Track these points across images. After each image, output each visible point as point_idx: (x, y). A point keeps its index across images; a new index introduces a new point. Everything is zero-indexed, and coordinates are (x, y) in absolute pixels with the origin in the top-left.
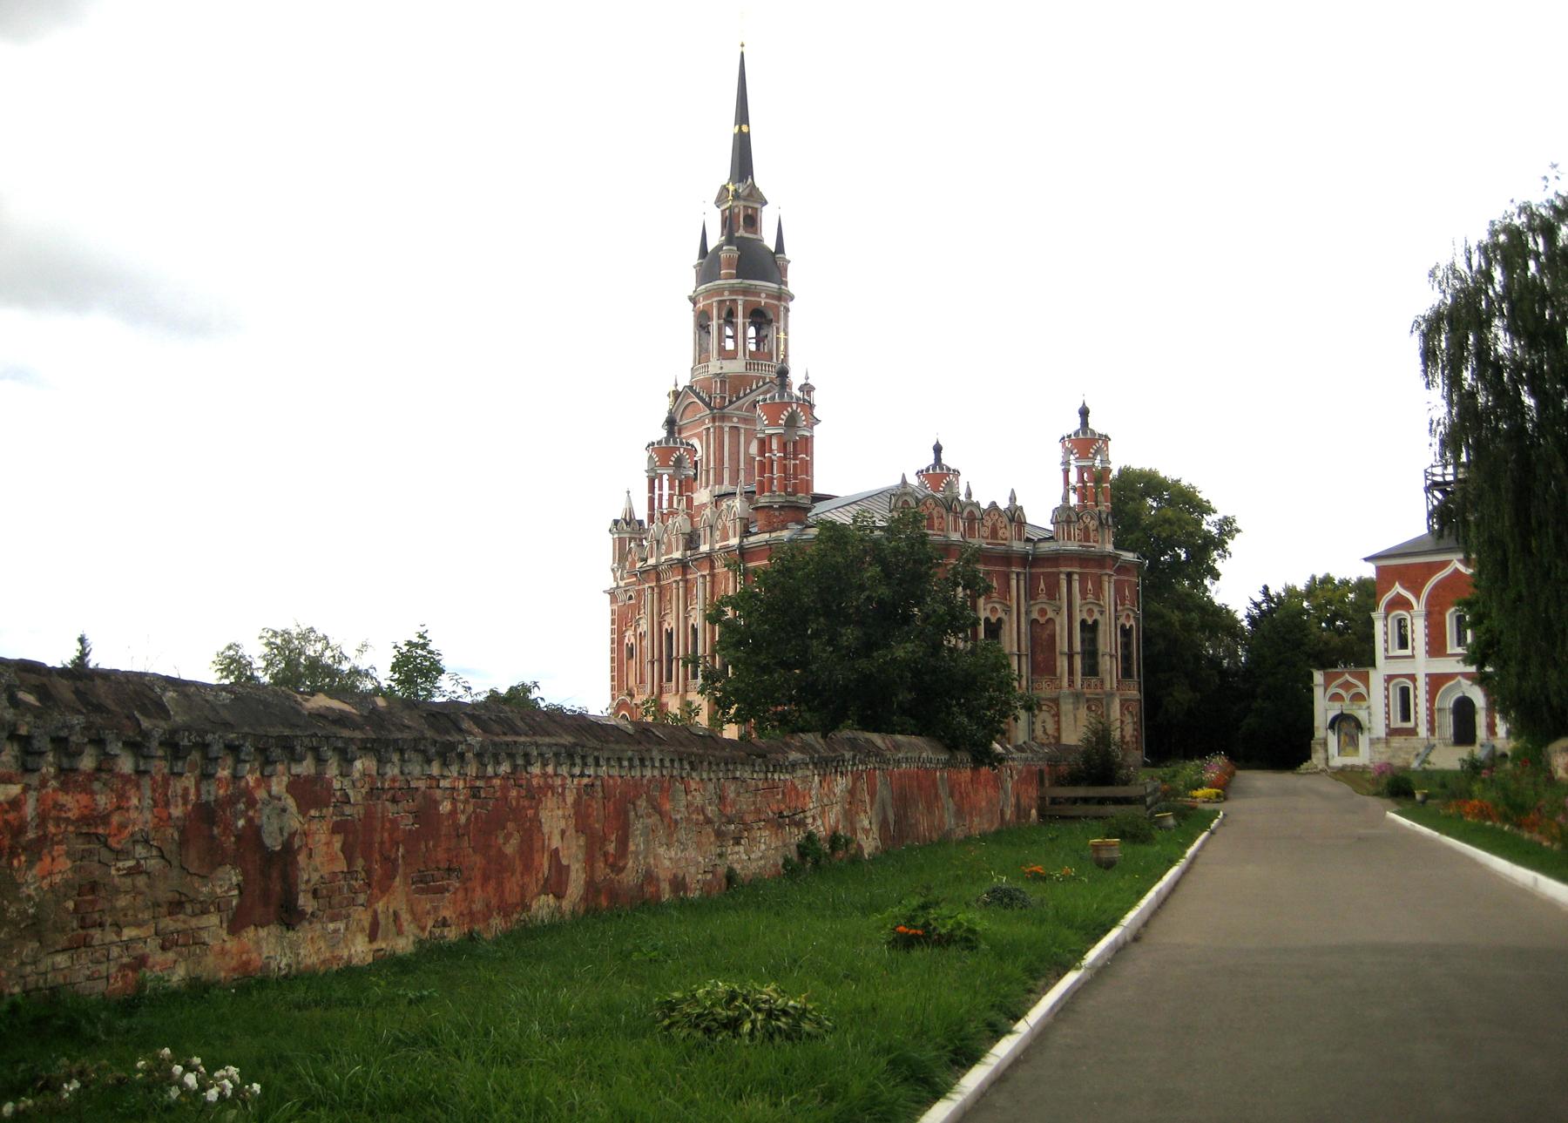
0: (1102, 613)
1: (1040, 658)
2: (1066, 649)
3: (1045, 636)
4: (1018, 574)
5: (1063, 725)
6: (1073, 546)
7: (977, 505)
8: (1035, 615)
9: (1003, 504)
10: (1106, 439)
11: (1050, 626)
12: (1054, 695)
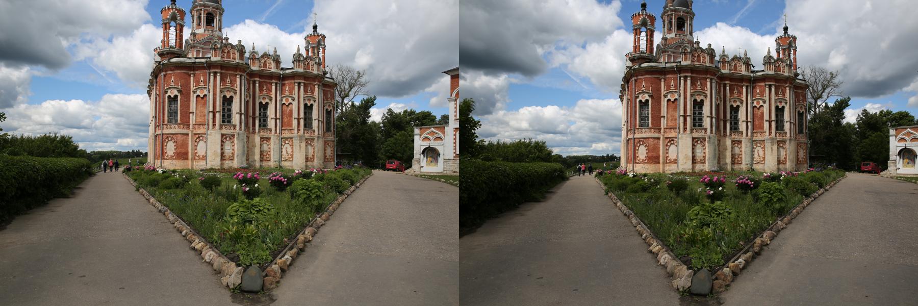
1: (757, 122)
4: (747, 87)
6: (772, 72)
7: (727, 56)
8: (755, 104)
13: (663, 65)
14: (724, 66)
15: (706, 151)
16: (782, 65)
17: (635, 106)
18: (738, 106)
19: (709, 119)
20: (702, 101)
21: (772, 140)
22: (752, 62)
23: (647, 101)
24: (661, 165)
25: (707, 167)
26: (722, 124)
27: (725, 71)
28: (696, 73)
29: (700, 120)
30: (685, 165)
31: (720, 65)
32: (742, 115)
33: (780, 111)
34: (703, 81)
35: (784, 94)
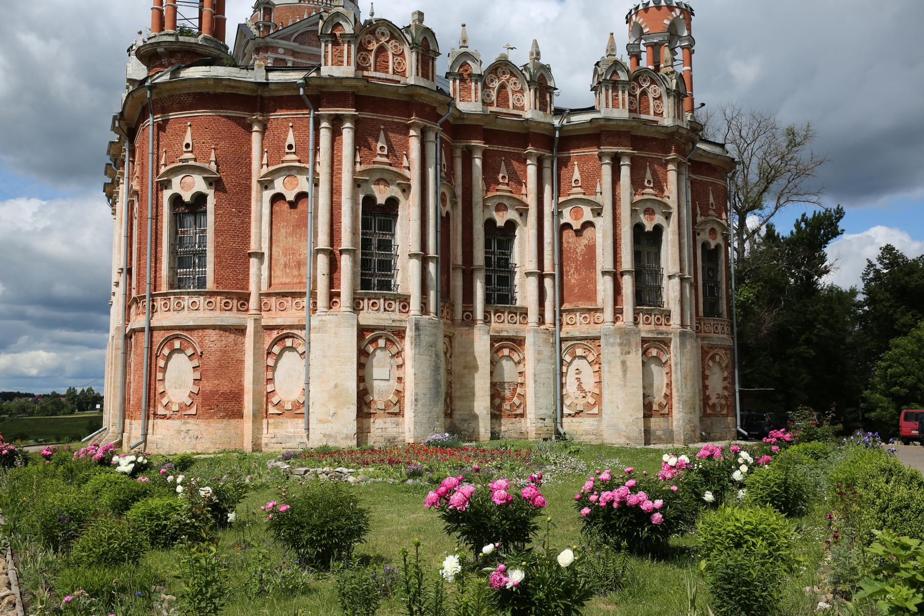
0: (667, 217)
1: (572, 278)
2: (609, 266)
3: (581, 248)
5: (606, 377)
6: (621, 113)
8: (567, 218)
9: (520, 58)
10: (688, 12)
11: (588, 232)
12: (593, 331)
13: (257, 75)
14: (465, 89)
15: (405, 373)
16: (653, 91)
17: (157, 217)
18: (511, 226)
19: (415, 265)
20: (393, 203)
21: (625, 334)
22: (558, 78)
23: (200, 198)
24: (247, 425)
25: (409, 428)
26: (458, 282)
27: (469, 105)
28: (375, 111)
29: (387, 266)
30: (333, 424)
31: (451, 87)
32: (523, 253)
33: (647, 241)
34: (395, 138)
35: (659, 186)
